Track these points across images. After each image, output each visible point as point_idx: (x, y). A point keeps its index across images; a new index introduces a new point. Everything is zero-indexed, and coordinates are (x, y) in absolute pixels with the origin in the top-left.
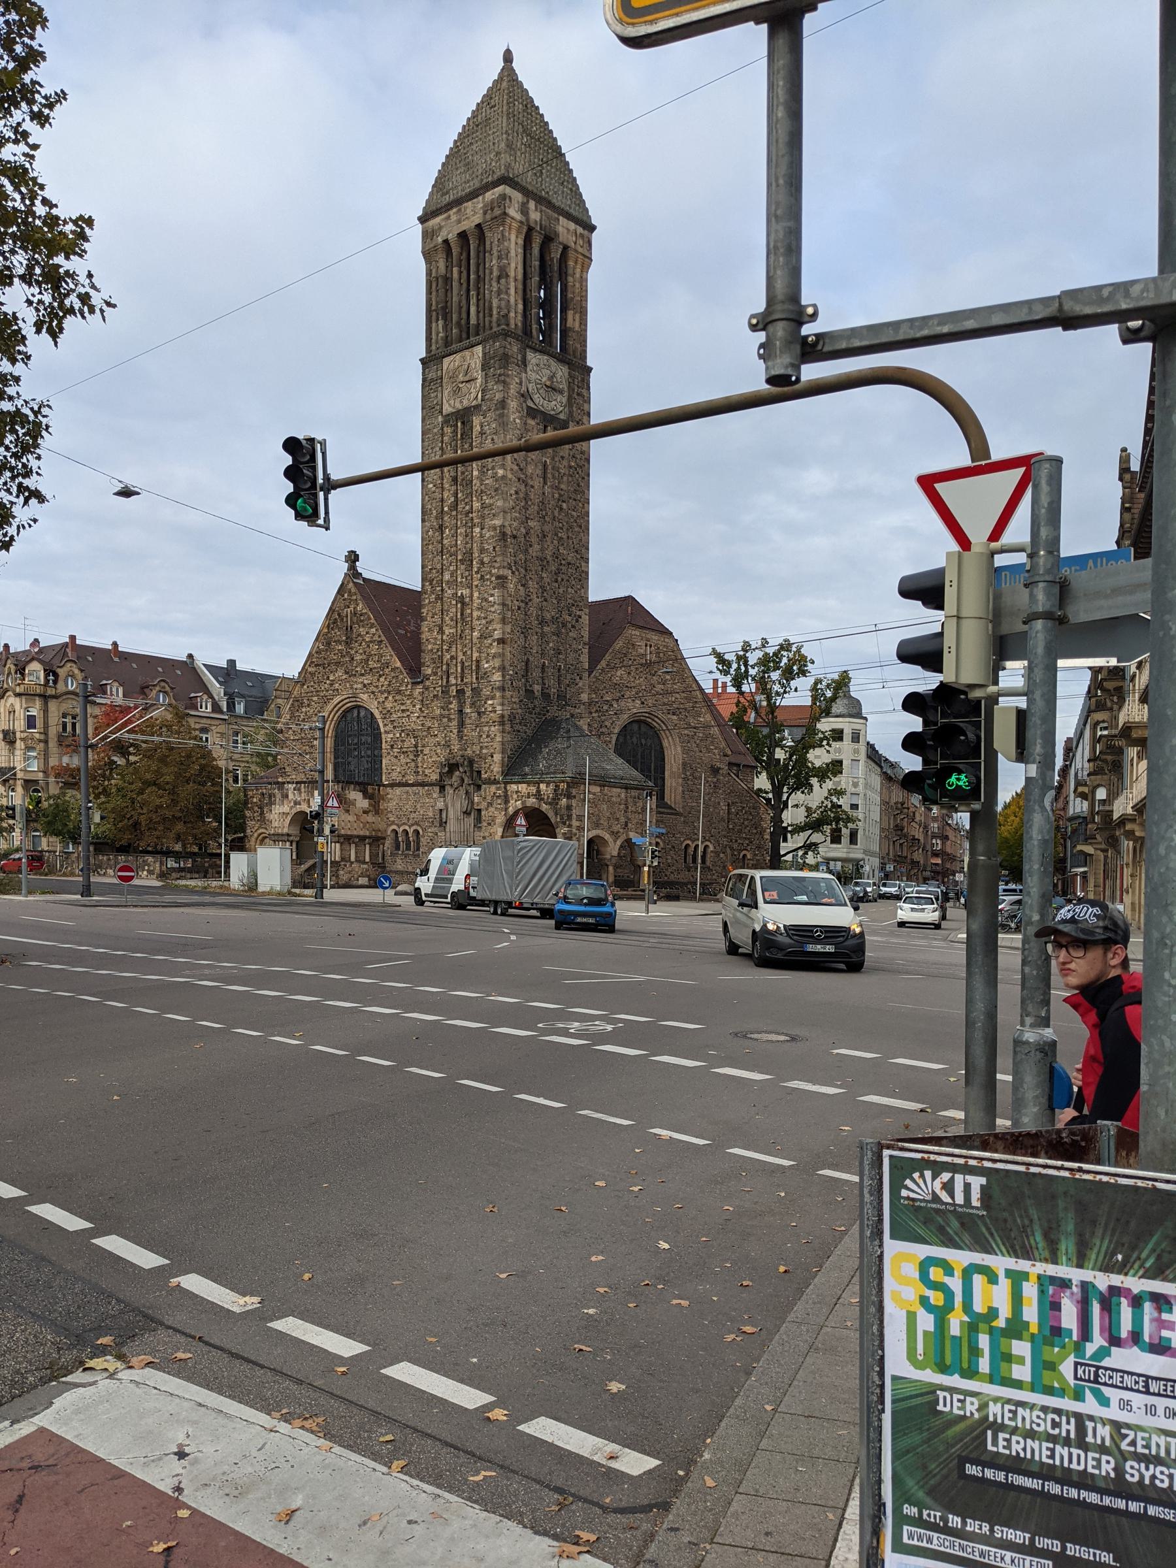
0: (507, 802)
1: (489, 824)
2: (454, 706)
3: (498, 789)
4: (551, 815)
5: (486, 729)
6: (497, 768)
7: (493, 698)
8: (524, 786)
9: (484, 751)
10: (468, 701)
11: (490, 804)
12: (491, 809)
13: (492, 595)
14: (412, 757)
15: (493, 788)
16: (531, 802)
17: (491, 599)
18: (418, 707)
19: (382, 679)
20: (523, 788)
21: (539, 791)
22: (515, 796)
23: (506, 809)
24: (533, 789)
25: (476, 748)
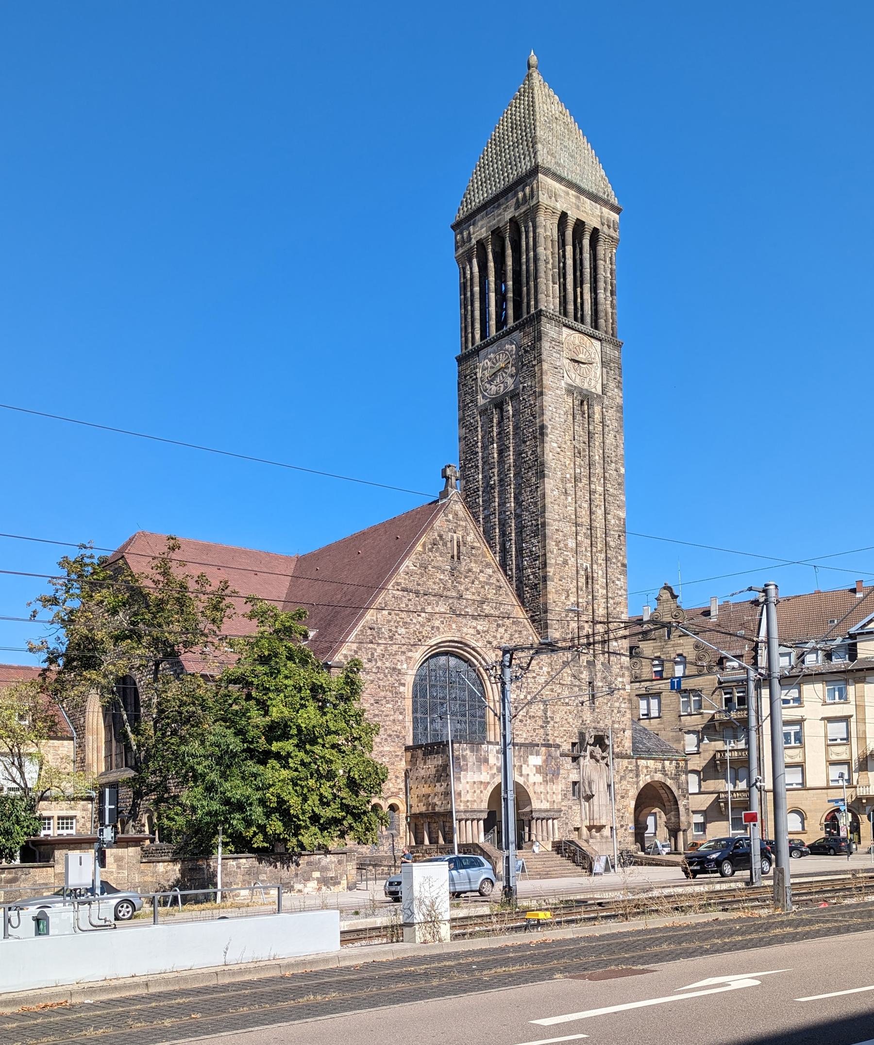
0: (637, 776)
1: (623, 797)
2: (585, 675)
3: (630, 763)
4: (674, 789)
5: (617, 704)
6: (628, 744)
7: (623, 676)
8: (652, 762)
9: (616, 726)
10: (599, 675)
11: (622, 778)
12: (624, 782)
13: (619, 579)
14: (541, 723)
15: (625, 762)
16: (658, 777)
17: (617, 582)
18: (545, 669)
19: (501, 630)
20: (651, 763)
21: (664, 767)
22: (645, 771)
23: (638, 783)
24: (659, 765)
25: (608, 722)
